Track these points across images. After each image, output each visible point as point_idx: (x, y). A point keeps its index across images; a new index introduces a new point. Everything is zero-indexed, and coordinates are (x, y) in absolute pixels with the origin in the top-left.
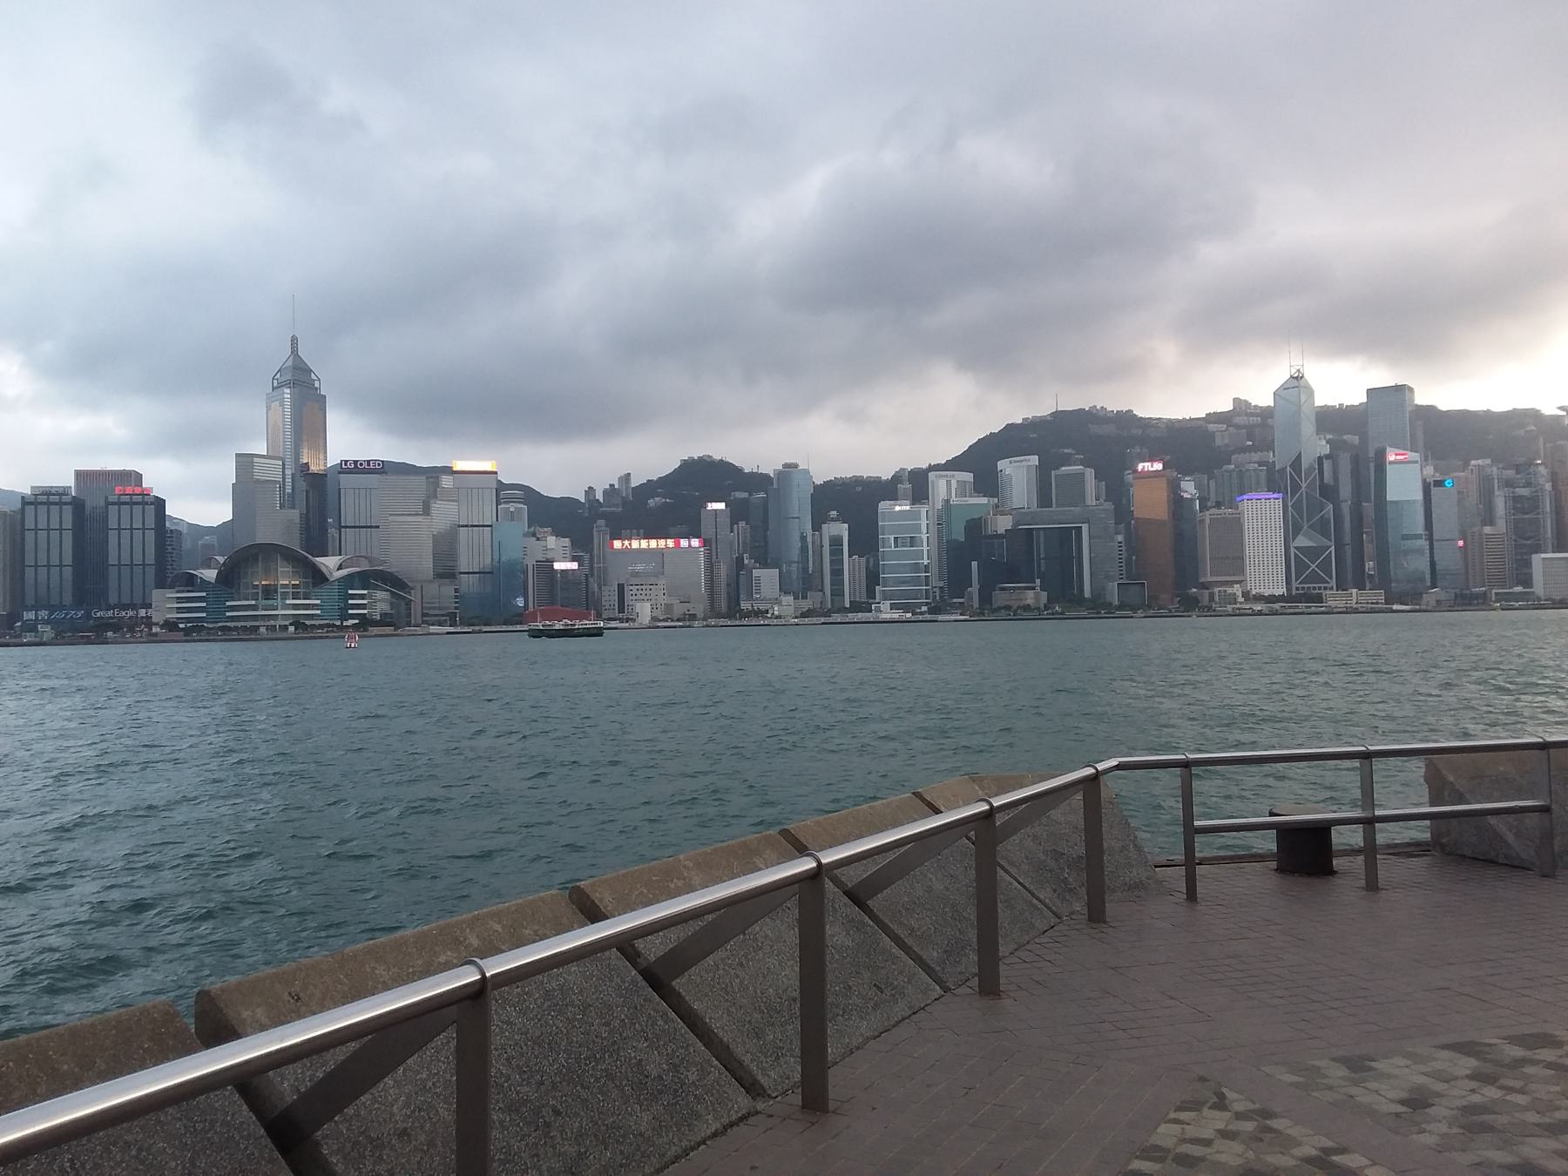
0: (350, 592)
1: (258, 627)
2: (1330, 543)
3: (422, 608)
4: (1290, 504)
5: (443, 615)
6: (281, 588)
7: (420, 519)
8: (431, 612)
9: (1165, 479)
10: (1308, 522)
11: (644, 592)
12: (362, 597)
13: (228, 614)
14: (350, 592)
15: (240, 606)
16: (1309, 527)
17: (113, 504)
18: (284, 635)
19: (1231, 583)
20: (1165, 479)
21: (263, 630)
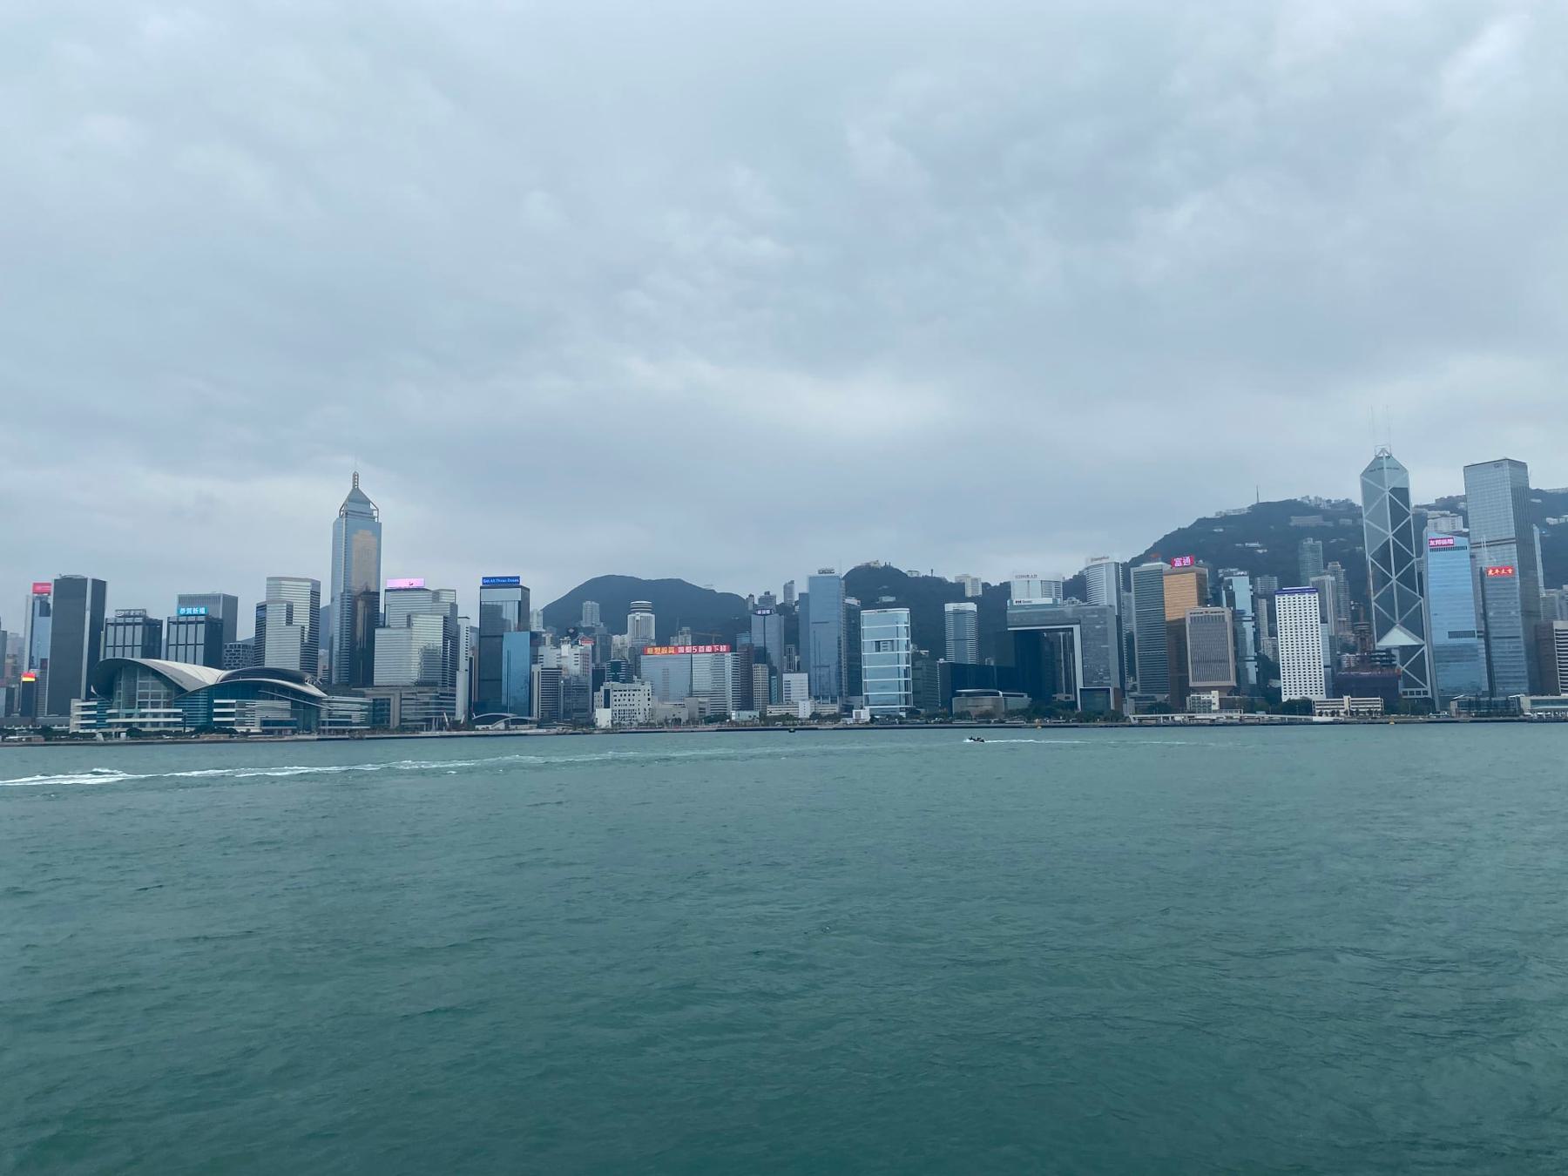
0: (215, 701)
1: (94, 734)
2: (1422, 642)
3: (401, 714)
4: (1373, 599)
5: (418, 721)
6: (139, 698)
7: (401, 632)
8: (409, 718)
9: (1194, 574)
10: (1400, 618)
11: (631, 697)
12: (232, 706)
13: (108, 721)
14: (215, 701)
15: (119, 715)
16: (1401, 624)
17: (174, 623)
18: (117, 741)
19: (1208, 690)
20: (1194, 574)
21: (100, 737)
